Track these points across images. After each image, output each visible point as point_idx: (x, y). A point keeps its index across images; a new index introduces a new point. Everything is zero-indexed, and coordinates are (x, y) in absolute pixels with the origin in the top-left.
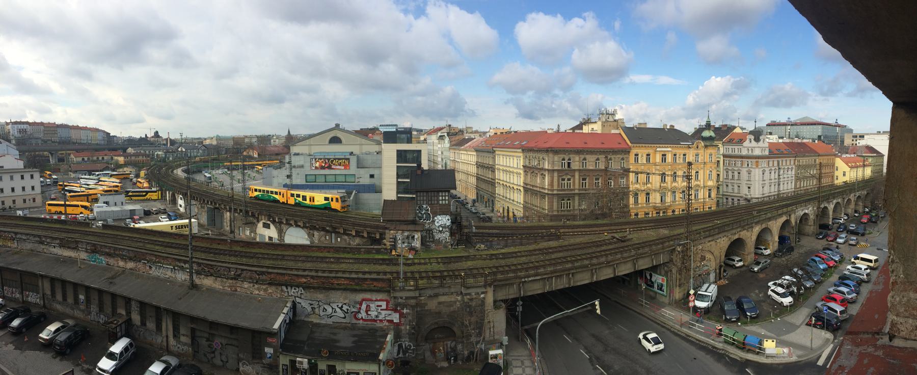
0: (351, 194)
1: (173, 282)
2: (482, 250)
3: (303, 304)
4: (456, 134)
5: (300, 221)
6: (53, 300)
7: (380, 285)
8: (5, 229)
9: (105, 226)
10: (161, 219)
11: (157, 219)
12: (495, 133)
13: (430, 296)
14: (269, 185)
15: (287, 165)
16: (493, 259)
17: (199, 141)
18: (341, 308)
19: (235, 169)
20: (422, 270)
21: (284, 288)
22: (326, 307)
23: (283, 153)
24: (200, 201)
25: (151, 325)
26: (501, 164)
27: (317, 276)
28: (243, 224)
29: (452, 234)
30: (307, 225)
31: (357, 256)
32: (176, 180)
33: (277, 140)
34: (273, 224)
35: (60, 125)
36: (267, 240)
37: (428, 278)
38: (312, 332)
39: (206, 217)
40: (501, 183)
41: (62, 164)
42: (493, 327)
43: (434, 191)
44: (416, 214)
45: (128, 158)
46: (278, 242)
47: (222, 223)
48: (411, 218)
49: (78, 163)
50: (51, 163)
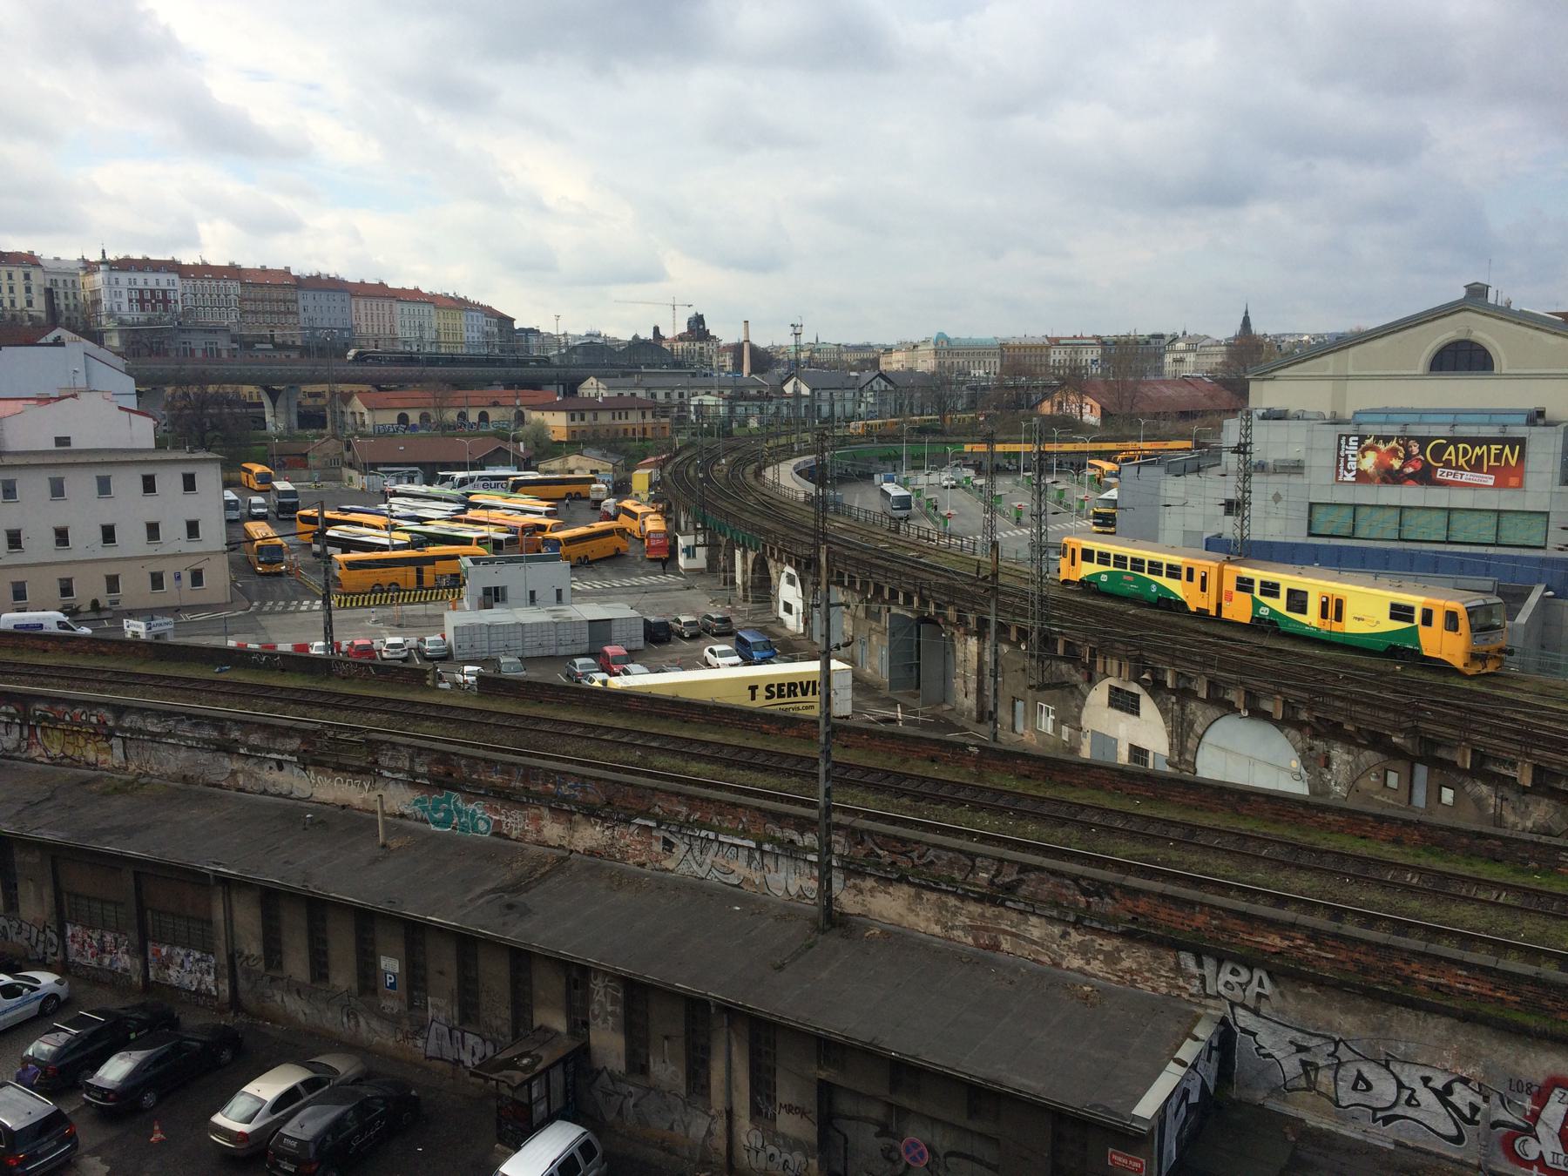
0: (1522, 597)
3: (1265, 1039)
5: (1270, 695)
6: (273, 979)
8: (74, 693)
9: (490, 685)
11: (698, 658)
14: (1143, 538)
15: (1231, 460)
17: (865, 356)
18: (1443, 1095)
21: (1188, 961)
22: (1369, 1071)
23: (1213, 412)
24: (863, 591)
25: (667, 1070)
27: (1336, 936)
28: (1031, 687)
30: (1304, 716)
31: (1536, 881)
32: (773, 507)
33: (1190, 358)
34: (1152, 695)
35: (310, 278)
36: (1123, 757)
41: (316, 436)
45: (583, 419)
46: (1168, 769)
47: (946, 678)
49: (382, 433)
50: (271, 429)
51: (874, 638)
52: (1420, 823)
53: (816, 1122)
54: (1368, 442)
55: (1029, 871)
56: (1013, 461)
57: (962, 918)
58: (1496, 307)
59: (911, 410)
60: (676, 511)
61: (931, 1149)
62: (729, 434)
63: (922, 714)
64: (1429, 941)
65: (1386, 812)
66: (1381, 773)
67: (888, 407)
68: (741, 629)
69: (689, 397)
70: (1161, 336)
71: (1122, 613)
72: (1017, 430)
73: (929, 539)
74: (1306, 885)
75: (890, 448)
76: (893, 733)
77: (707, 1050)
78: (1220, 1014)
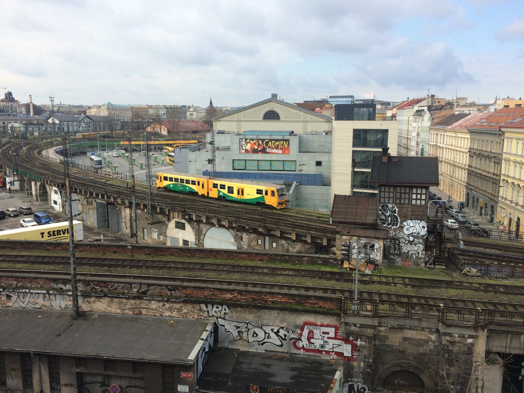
0: (290, 185)
1: (47, 313)
2: (472, 276)
3: (227, 327)
4: (441, 108)
5: (224, 220)
7: (328, 305)
10: (23, 223)
12: (505, 106)
13: (393, 328)
15: (209, 146)
16: (490, 291)
17: (81, 109)
18: (277, 333)
19: (136, 151)
20: (382, 291)
21: (203, 306)
22: (257, 330)
24: (85, 194)
26: (514, 152)
28: (149, 224)
29: (427, 248)
30: (234, 225)
31: (297, 267)
32: (46, 165)
33: (195, 114)
36: (181, 244)
37: (391, 303)
38: (238, 363)
39: (95, 216)
40: (510, 180)
42: (483, 387)
43: (396, 186)
44: (378, 215)
46: (195, 246)
47: (118, 224)
48: (370, 220)
51: (91, 211)
52: (267, 254)
53: (77, 387)
54: (248, 141)
55: (151, 286)
56: (139, 147)
57: (128, 306)
58: (279, 101)
59: (100, 129)
60: (5, 168)
61: (120, 387)
62: (26, 138)
63: (111, 237)
64: (271, 288)
65: (258, 252)
66: (256, 240)
67: (91, 128)
68: (36, 212)
69: (7, 124)
70: (185, 106)
71: (178, 197)
72: (139, 137)
73: (109, 175)
74: (237, 277)
75: (92, 143)
76: (99, 245)
77: (31, 371)
78: (214, 321)
